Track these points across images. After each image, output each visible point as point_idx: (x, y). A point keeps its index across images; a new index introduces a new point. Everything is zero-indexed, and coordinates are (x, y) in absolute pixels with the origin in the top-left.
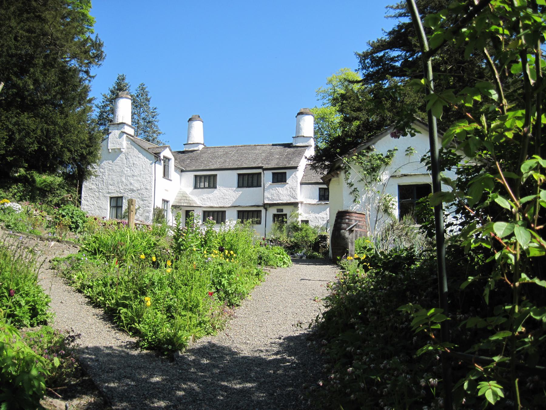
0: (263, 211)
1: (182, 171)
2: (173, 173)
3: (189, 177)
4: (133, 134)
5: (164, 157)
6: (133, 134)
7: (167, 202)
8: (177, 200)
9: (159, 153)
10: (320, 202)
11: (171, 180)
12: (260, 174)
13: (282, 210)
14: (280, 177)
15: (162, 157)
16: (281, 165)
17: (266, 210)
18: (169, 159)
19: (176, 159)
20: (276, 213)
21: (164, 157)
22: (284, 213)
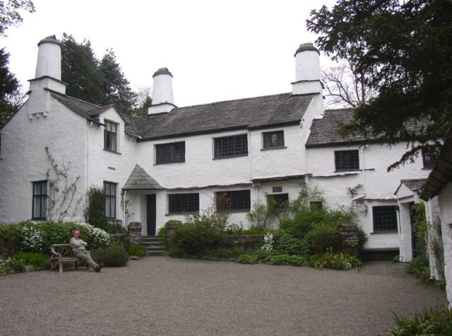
1: (138, 141)
2: (122, 141)
3: (149, 150)
4: (64, 93)
5: (105, 120)
6: (64, 93)
7: (115, 184)
8: (131, 182)
9: (97, 116)
11: (120, 154)
12: (245, 136)
14: (274, 141)
15: (102, 121)
16: (275, 121)
18: (116, 124)
19: (126, 125)
20: (271, 192)
21: (105, 120)
22: (284, 191)
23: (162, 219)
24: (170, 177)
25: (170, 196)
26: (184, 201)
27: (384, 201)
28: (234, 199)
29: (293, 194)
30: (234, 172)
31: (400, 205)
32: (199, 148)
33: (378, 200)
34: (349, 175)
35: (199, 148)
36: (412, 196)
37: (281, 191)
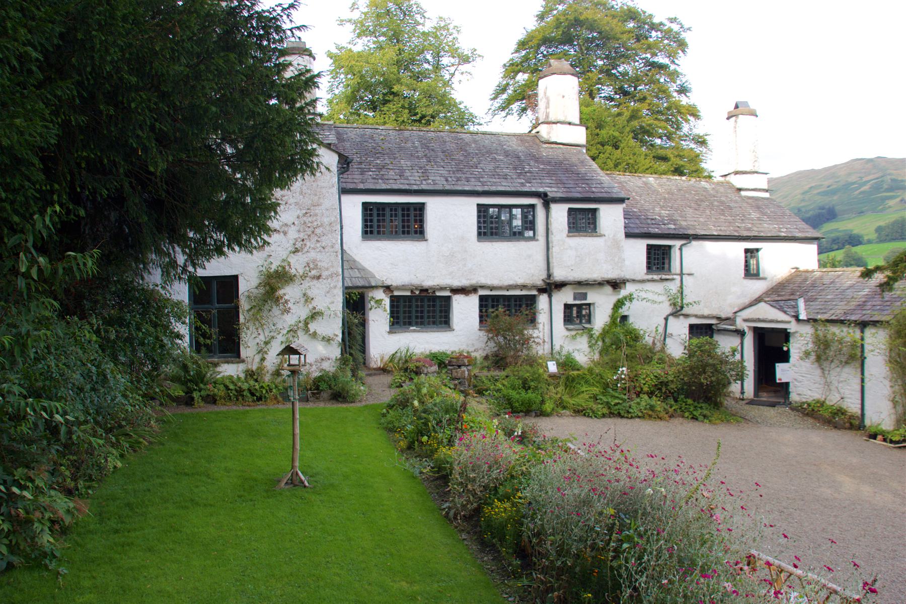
0: (543, 300)
10: (650, 277)
13: (584, 296)
17: (550, 297)
20: (571, 301)
23: (384, 341)
24: (395, 263)
25: (395, 301)
26: (422, 307)
27: (703, 317)
28: (506, 309)
29: (602, 306)
30: (510, 264)
31: (746, 330)
32: (451, 218)
33: (696, 316)
34: (667, 280)
35: (451, 218)
36: (789, 322)
37: (586, 299)
